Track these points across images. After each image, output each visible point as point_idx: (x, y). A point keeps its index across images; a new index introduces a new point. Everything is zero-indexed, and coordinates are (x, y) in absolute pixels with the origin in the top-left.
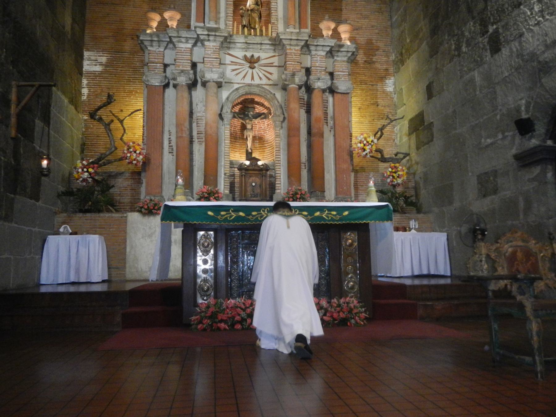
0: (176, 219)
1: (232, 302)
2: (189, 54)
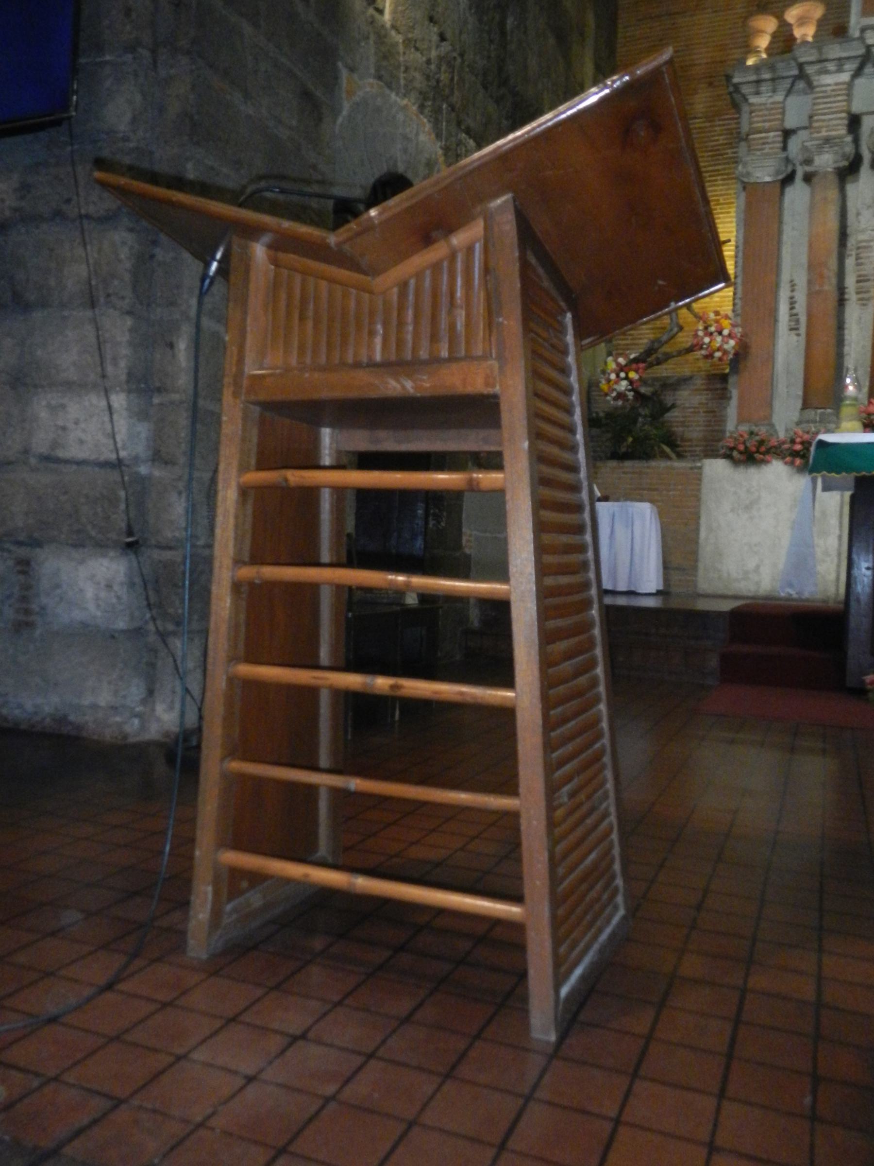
2: (845, 98)
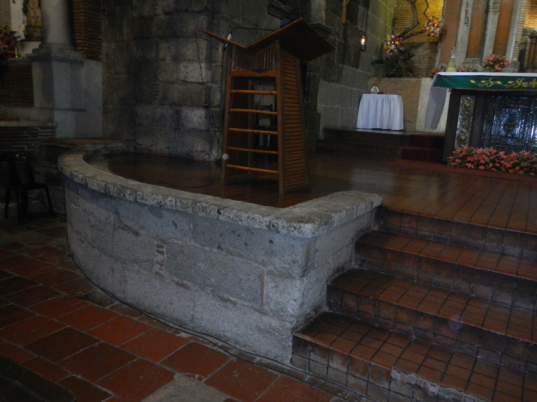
1: (480, 150)
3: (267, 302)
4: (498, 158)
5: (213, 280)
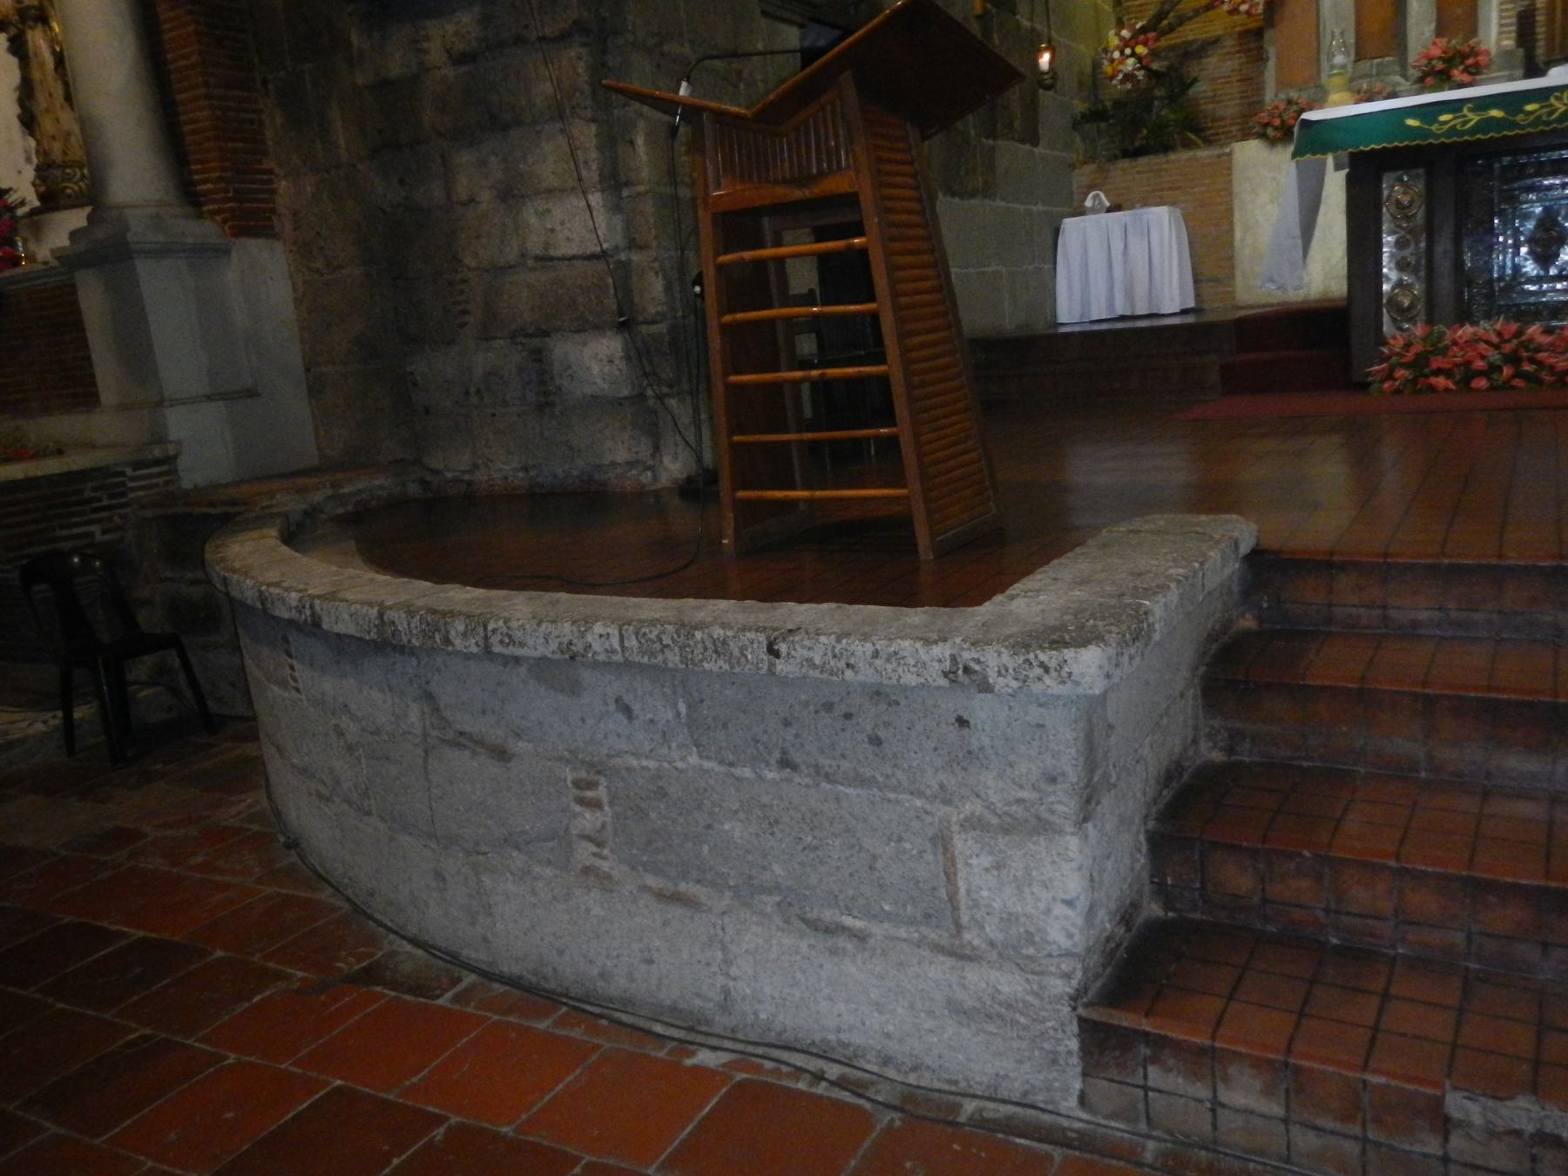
0: (1324, 148)
1: (1467, 331)
3: (973, 919)
4: (1525, 345)
5: (777, 869)
